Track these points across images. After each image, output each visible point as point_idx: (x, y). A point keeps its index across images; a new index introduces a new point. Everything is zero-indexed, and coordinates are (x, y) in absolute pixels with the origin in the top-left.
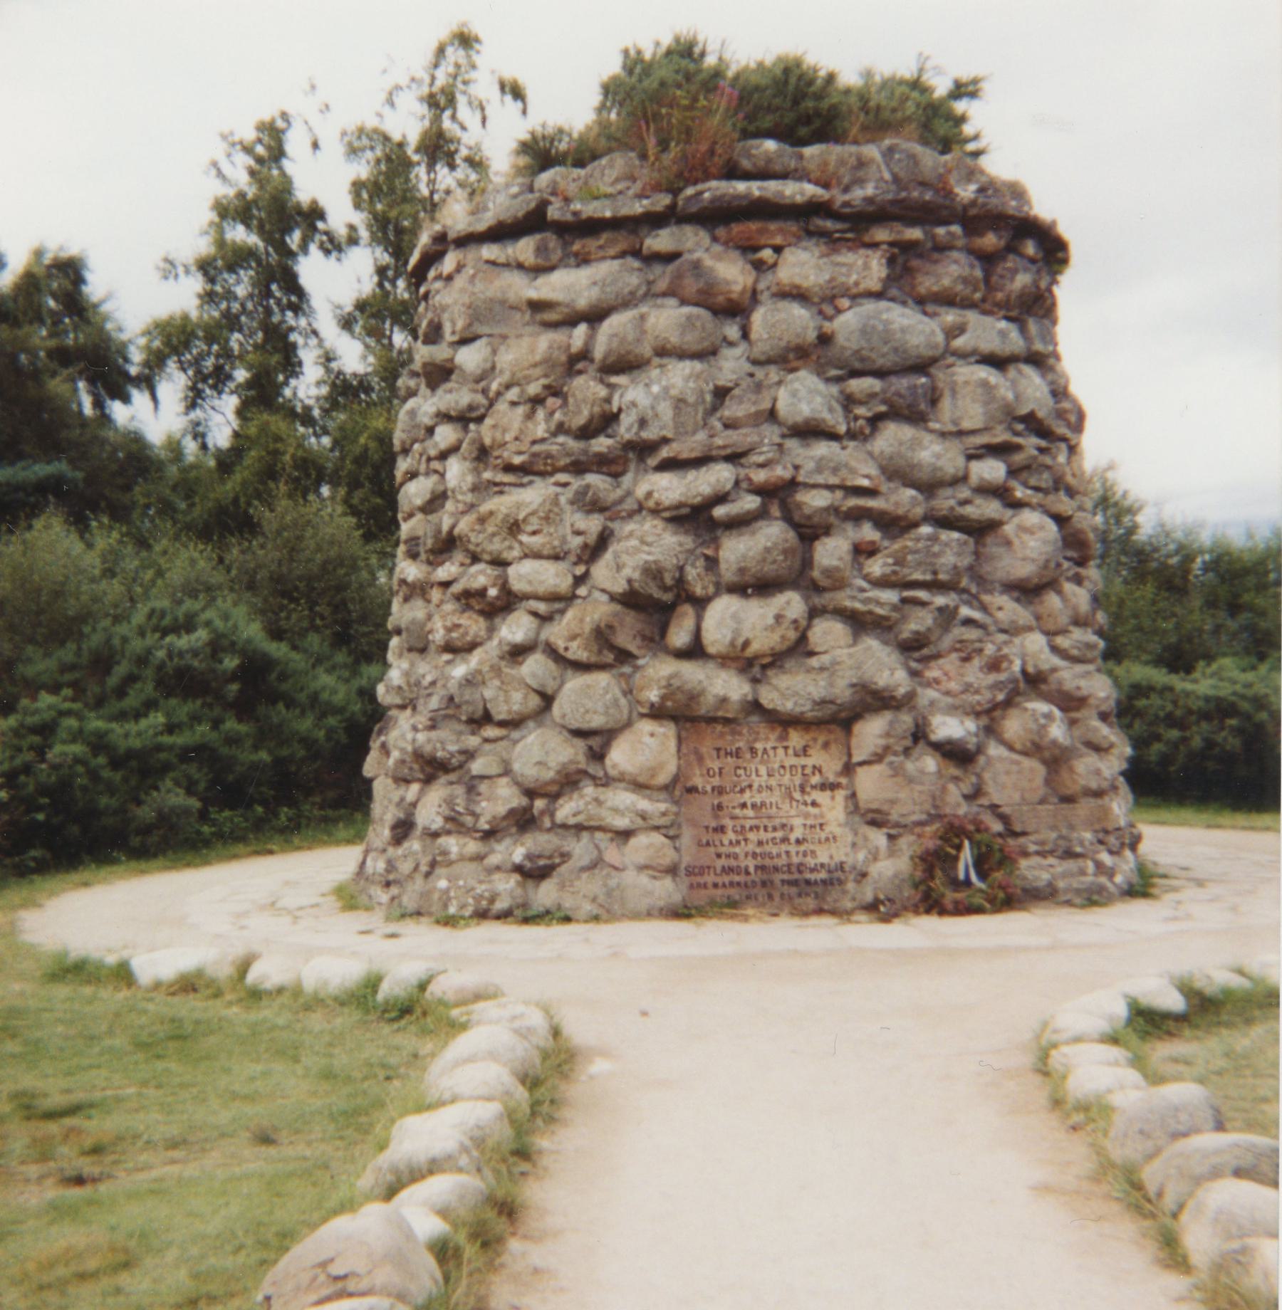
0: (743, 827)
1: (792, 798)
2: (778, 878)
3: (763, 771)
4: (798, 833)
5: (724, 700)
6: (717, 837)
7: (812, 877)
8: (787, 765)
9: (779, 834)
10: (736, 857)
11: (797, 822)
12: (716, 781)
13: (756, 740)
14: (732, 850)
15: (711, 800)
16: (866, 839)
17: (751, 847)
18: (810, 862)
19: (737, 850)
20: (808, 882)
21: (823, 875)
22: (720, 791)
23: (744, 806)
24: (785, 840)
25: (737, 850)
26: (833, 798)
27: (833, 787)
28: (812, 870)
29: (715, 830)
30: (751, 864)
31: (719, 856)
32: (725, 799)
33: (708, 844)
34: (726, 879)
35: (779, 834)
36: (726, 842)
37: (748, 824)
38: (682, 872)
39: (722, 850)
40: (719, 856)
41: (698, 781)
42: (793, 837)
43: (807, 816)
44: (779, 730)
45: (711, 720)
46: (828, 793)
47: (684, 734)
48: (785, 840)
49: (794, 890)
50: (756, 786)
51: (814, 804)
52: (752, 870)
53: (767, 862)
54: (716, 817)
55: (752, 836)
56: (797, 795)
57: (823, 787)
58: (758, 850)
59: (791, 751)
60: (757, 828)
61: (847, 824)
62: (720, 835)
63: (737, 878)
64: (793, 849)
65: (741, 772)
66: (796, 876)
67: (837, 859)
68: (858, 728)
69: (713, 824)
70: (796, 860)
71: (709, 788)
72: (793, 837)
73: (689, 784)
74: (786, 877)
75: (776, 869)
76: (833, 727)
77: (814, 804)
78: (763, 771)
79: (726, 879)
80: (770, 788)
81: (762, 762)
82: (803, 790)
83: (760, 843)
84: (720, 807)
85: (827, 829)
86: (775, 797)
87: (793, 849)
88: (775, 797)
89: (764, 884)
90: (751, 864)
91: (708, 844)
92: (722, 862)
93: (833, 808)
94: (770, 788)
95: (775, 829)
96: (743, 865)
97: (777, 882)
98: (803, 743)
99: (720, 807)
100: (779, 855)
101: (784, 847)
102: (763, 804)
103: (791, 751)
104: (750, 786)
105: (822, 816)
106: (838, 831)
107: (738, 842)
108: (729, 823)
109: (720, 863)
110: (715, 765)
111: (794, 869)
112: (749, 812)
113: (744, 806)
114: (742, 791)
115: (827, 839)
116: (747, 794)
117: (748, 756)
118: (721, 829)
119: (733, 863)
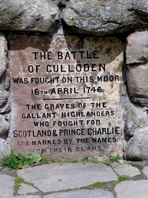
0: (52, 105)
1: (85, 86)
2: (75, 137)
3: (66, 68)
4: (88, 109)
5: (38, 19)
6: (34, 112)
7: (97, 137)
8: (82, 64)
9: (76, 110)
10: (47, 124)
11: (88, 101)
12: (34, 74)
13: (61, 47)
14: (45, 120)
15: (29, 88)
16: (133, 114)
17: (57, 118)
18: (96, 127)
19: (48, 120)
20: (94, 140)
21: (104, 136)
22: (36, 81)
23: (53, 91)
24: (80, 113)
25: (48, 120)
26: (112, 86)
27: (112, 78)
28: (97, 133)
29: (34, 107)
30: (57, 129)
31: (36, 124)
32: (40, 87)
33: (29, 116)
34: (41, 139)
35: (76, 110)
36: (41, 116)
37: (55, 103)
38: (11, 134)
39: (38, 120)
40: (36, 124)
41: (22, 75)
42: (85, 112)
43: (94, 98)
44: (77, 40)
45: (29, 33)
46: (109, 82)
47: (12, 42)
48: (80, 113)
49: (85, 145)
50: (61, 78)
51: (99, 90)
52: (58, 132)
53: (68, 127)
54: (34, 99)
55: (57, 111)
56: (88, 84)
57: (106, 79)
58: (62, 120)
59: (85, 55)
60: (62, 106)
61: (121, 102)
62: (36, 111)
63: (48, 139)
64: (85, 119)
65: (49, 68)
66: (87, 136)
67: (113, 125)
68: (131, 38)
69: (32, 103)
70: (86, 126)
71: (29, 80)
72: (85, 112)
73: (16, 77)
74: (80, 137)
75: (74, 132)
76: (113, 38)
77: (99, 90)
78: (66, 68)
79: (41, 139)
80: (70, 79)
81: (64, 62)
82: (92, 81)
83: (63, 115)
84: (37, 92)
85: (108, 106)
86: (74, 86)
87: (85, 119)
88: (74, 86)
89: (66, 141)
90: (57, 129)
91: (29, 116)
92: (38, 128)
93: (113, 93)
94: (70, 79)
95: (73, 106)
96: (52, 130)
97: (74, 140)
98: (93, 49)
99: (37, 92)
100: (76, 123)
101: (79, 118)
102: (66, 90)
103: (85, 55)
104: (58, 78)
105: (105, 98)
106: (114, 107)
107: (49, 115)
108: (43, 103)
109: (36, 129)
110: (34, 64)
111: (85, 132)
112: (57, 96)
113: (53, 91)
114: (52, 81)
115: (108, 113)
116: (56, 83)
117: (56, 58)
118: (38, 106)
119: (45, 128)
